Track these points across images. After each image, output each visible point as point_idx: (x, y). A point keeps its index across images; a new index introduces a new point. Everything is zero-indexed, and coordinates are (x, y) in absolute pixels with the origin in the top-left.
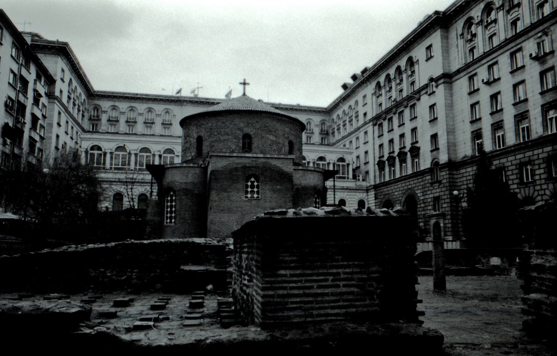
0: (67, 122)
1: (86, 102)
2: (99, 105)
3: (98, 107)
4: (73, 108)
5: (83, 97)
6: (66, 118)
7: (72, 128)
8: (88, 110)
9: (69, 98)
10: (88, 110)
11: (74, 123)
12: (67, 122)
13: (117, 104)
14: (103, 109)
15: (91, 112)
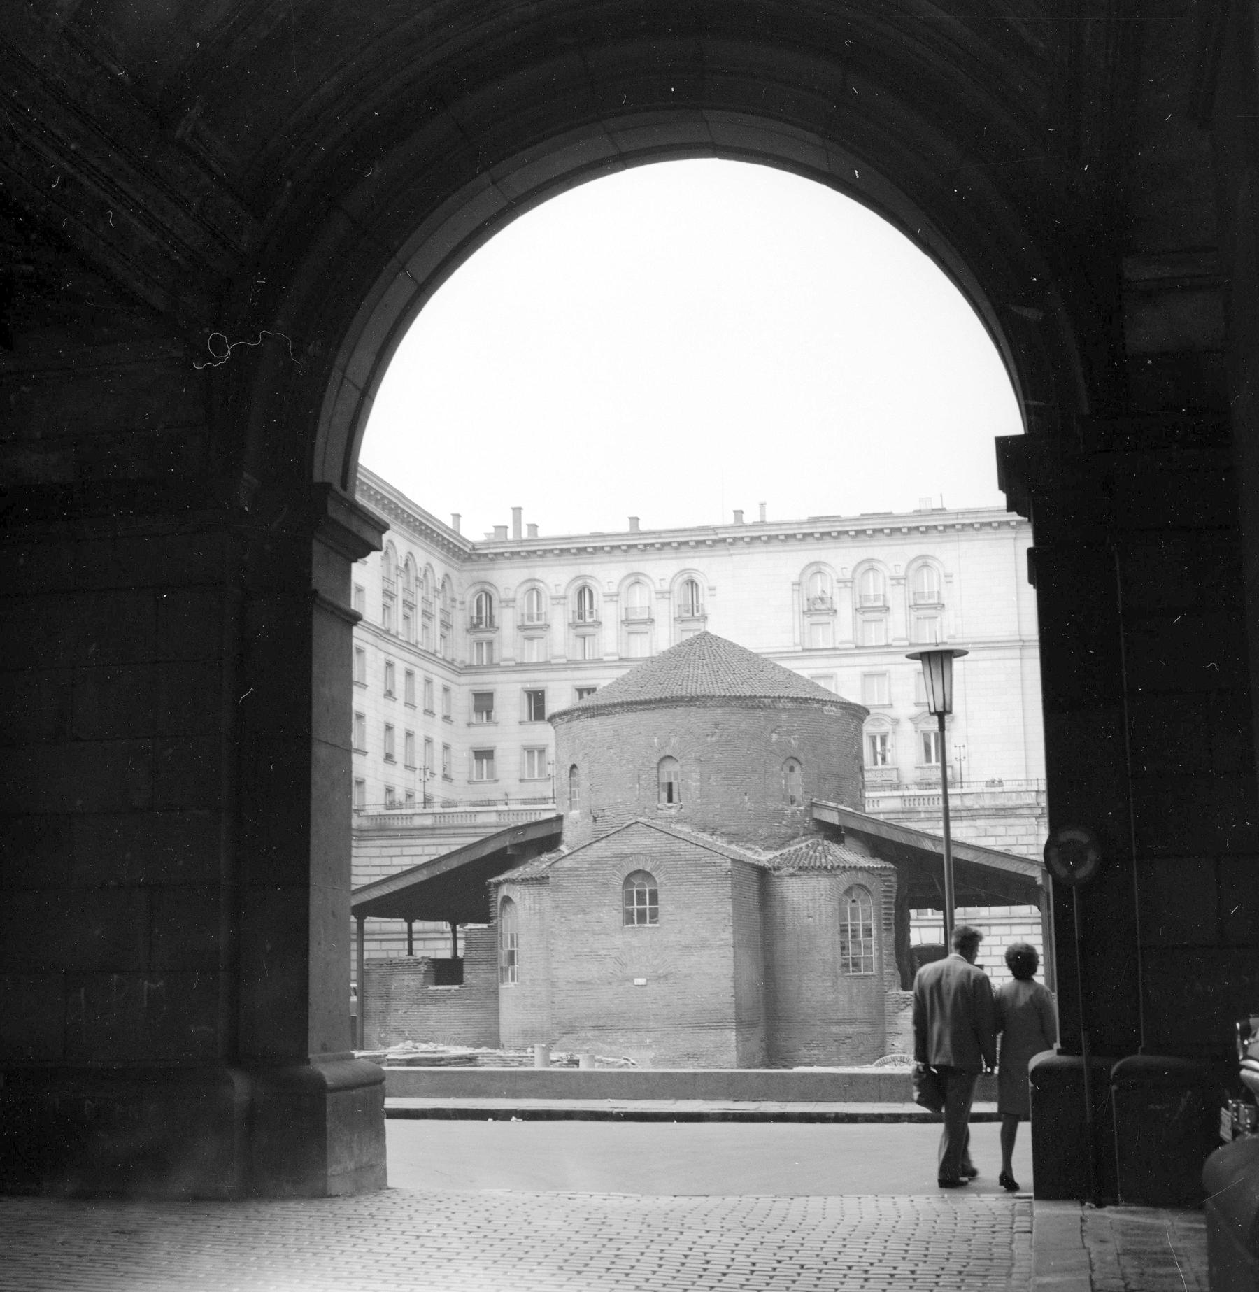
0: (389, 665)
1: (454, 581)
2: (491, 584)
3: (487, 587)
4: (406, 617)
5: (439, 569)
6: (382, 656)
7: (409, 674)
8: (463, 603)
9: (389, 594)
10: (463, 603)
11: (413, 658)
12: (389, 665)
13: (539, 573)
14: (503, 597)
15: (471, 608)
